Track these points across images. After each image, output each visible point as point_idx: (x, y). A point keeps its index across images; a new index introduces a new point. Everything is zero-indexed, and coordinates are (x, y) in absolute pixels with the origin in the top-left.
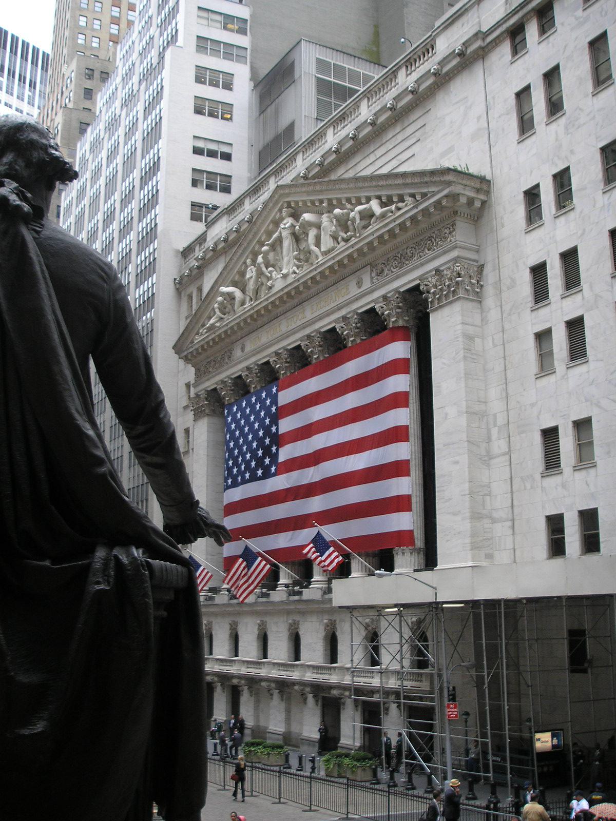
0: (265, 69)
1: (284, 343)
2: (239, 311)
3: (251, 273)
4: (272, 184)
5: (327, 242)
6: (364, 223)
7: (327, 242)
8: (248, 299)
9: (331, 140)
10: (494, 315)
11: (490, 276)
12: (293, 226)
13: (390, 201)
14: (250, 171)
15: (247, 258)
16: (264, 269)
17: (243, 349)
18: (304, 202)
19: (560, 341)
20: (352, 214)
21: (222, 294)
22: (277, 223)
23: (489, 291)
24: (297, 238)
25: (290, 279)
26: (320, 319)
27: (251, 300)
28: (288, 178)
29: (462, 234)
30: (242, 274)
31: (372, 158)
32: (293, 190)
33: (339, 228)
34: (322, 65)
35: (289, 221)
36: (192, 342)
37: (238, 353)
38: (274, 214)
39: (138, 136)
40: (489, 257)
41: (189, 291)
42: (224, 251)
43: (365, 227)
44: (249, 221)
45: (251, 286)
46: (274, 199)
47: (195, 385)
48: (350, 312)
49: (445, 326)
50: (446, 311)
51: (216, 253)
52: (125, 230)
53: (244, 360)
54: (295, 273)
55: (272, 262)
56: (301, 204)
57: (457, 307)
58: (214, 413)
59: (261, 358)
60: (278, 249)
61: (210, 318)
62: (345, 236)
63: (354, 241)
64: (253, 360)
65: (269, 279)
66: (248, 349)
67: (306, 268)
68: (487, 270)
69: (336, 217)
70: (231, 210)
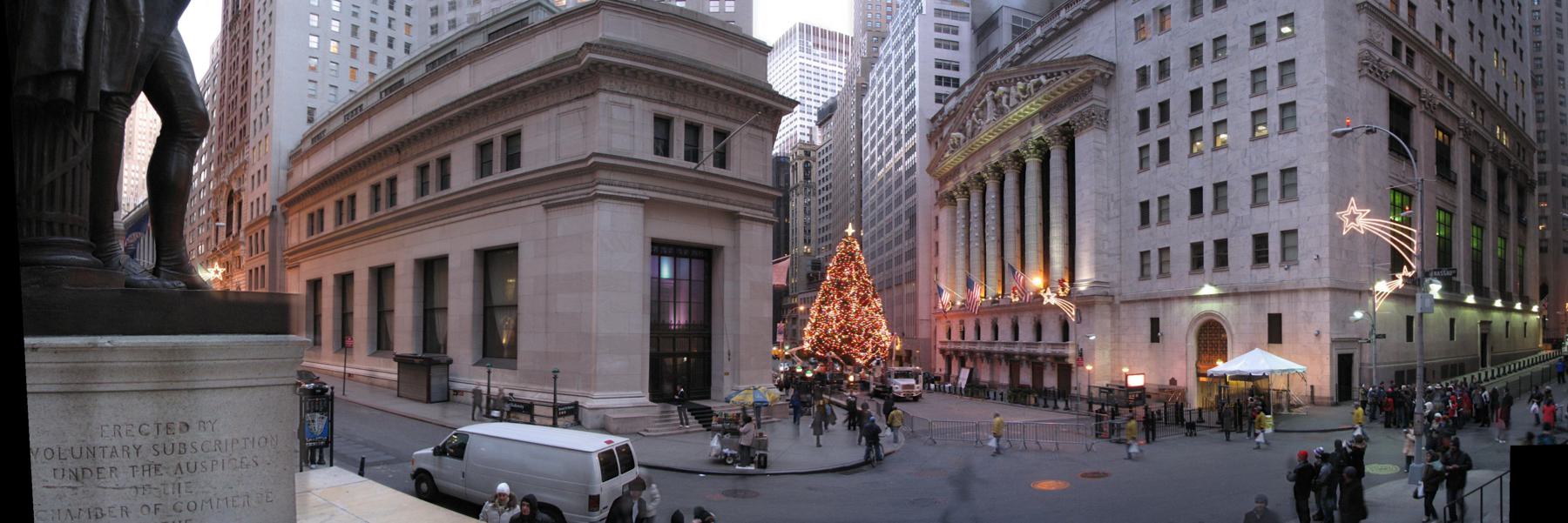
0: (979, 23)
3: (969, 124)
9: (1018, 48)
10: (1115, 137)
11: (1113, 116)
13: (1052, 75)
19: (1154, 152)
22: (983, 95)
23: (1112, 124)
24: (996, 101)
29: (1098, 91)
40: (1113, 105)
45: (969, 130)
51: (950, 117)
52: (898, 112)
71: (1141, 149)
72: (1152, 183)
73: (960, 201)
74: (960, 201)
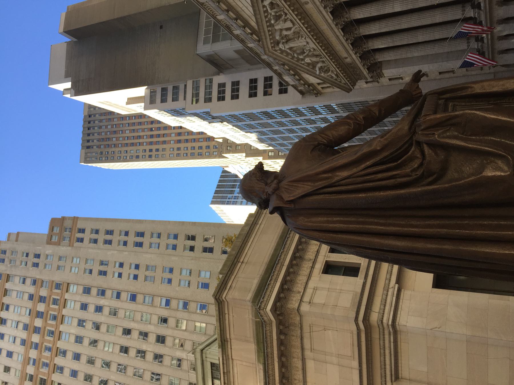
0: (213, 69)
1: (341, 38)
2: (327, 63)
3: (308, 60)
4: (264, 57)
5: (289, 24)
6: (276, 6)
7: (289, 24)
8: (321, 60)
12: (283, 43)
14: (260, 68)
15: (301, 64)
16: (306, 54)
17: (346, 58)
18: (270, 39)
20: (273, 14)
21: (320, 73)
22: (282, 52)
24: (288, 40)
25: (309, 40)
26: (327, 20)
27: (321, 58)
28: (259, 50)
30: (308, 64)
31: (244, 8)
32: (266, 46)
33: (281, 19)
34: (206, 42)
35: (281, 46)
36: (345, 84)
37: (348, 60)
38: (278, 53)
39: (253, 123)
41: (320, 89)
42: (299, 75)
43: (278, 5)
44: (284, 65)
45: (314, 59)
46: (272, 55)
47: (366, 78)
48: (322, 5)
53: (351, 56)
54: (305, 38)
55: (302, 51)
56: (272, 41)
58: (380, 68)
59: (349, 48)
60: (295, 49)
61: (332, 77)
62: (284, 16)
63: (286, 11)
64: (351, 52)
65: (310, 51)
66: (346, 55)
67: (302, 33)
69: (275, 22)
70: (280, 75)
73: (380, 58)
74: (380, 58)
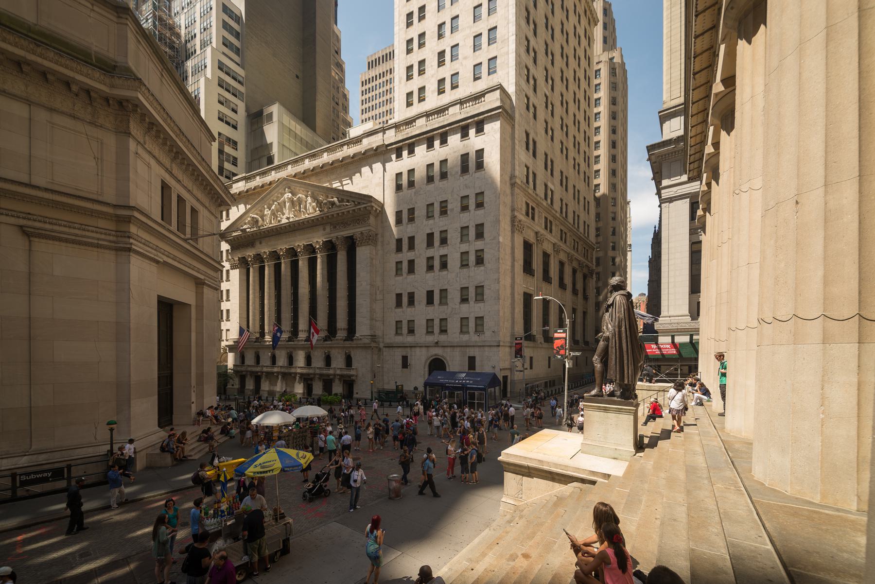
11: (380, 239)
19: (405, 265)
23: (379, 243)
49: (363, 253)
50: (363, 248)
57: (368, 247)
68: (379, 236)
71: (397, 263)
72: (404, 284)
